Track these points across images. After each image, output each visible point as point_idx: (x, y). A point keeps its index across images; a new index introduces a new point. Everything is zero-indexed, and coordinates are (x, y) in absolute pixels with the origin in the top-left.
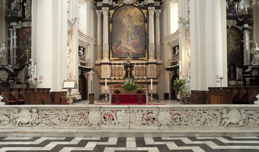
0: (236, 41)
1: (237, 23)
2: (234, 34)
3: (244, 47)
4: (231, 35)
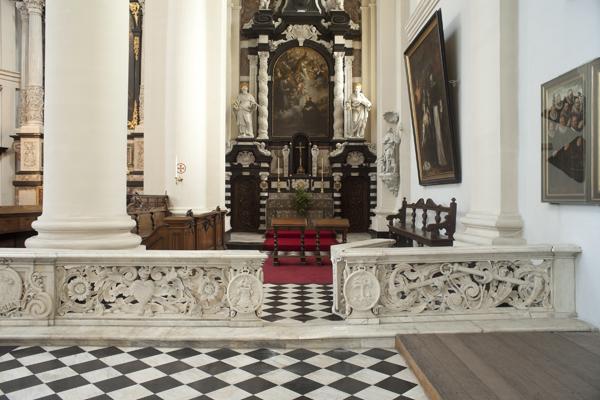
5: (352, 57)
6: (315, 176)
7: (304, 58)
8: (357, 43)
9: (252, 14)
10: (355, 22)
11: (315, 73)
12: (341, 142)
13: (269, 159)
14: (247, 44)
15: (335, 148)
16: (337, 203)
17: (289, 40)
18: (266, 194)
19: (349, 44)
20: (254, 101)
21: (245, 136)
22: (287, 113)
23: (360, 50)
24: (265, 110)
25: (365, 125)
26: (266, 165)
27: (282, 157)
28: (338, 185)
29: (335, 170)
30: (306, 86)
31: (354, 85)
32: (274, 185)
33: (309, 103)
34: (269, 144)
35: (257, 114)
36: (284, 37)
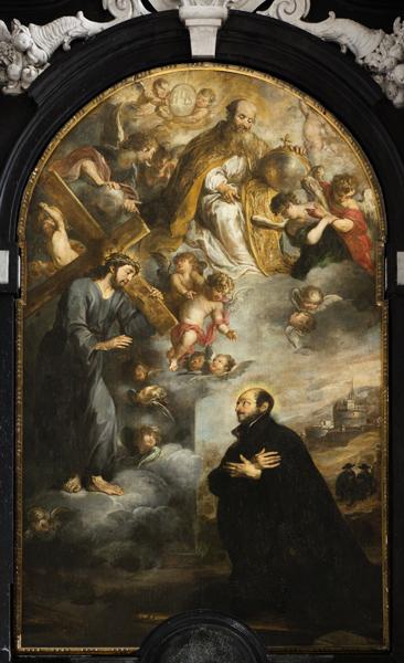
0: (319, 275)
2: (278, 157)
4: (235, 165)
7: (222, 136)
11: (296, 233)
17: (122, 15)
33: (257, 431)
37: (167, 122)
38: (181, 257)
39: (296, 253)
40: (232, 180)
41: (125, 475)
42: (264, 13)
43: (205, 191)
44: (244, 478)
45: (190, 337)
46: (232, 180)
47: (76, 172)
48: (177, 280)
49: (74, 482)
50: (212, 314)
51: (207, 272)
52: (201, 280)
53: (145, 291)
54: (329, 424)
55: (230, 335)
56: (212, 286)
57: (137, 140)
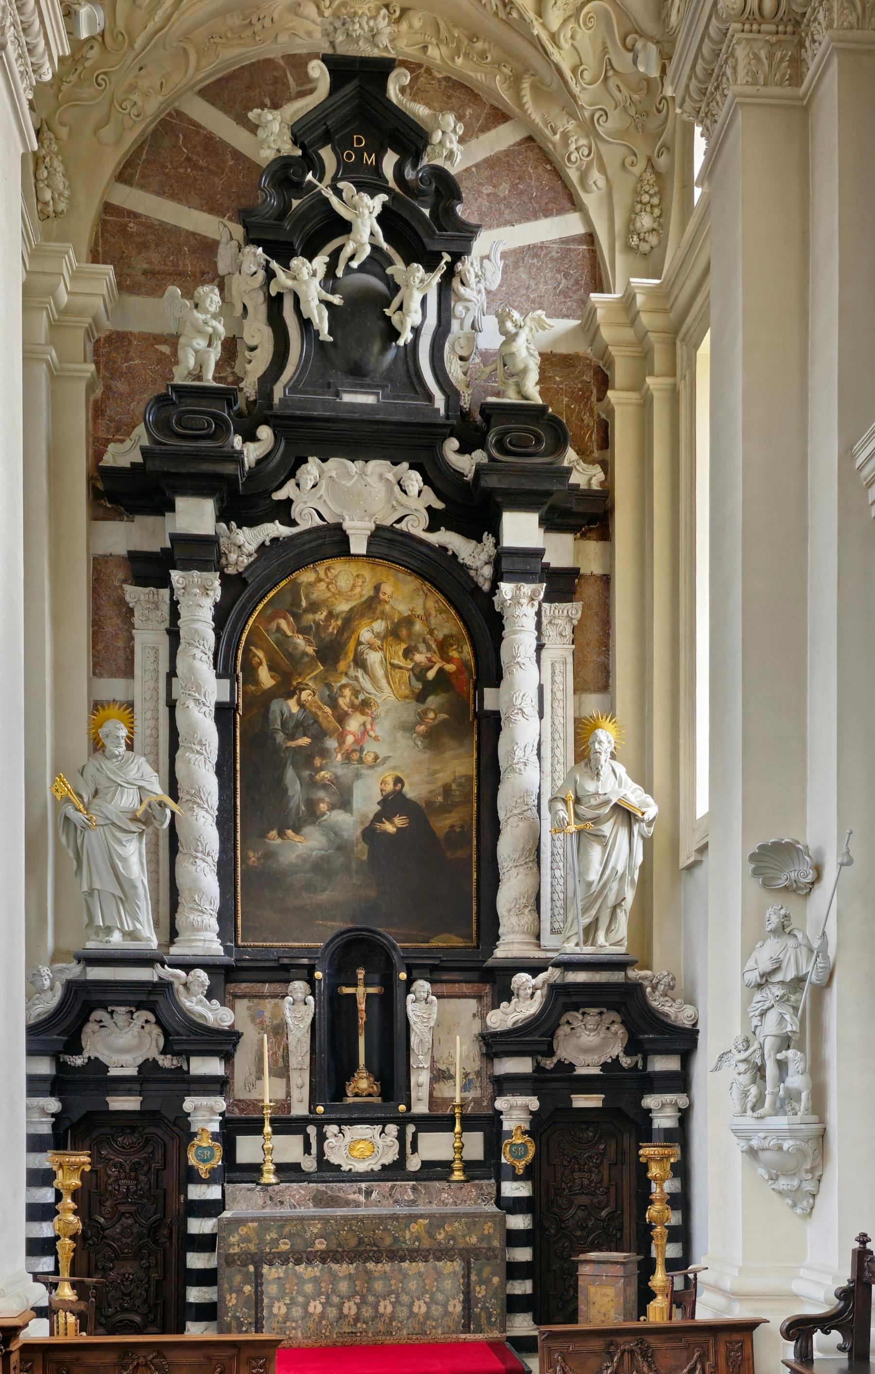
0: (432, 701)
1: (439, 505)
2: (408, 621)
3: (503, 764)
4: (379, 626)
5: (573, 610)
6: (420, 1108)
7: (371, 606)
8: (593, 547)
9: (140, 404)
10: (582, 453)
11: (419, 673)
12: (535, 970)
13: (224, 1043)
14: (125, 536)
15: (505, 994)
16: (519, 1222)
17: (304, 525)
18: (214, 1193)
19: (560, 550)
20: (157, 788)
21: (116, 938)
22: (302, 846)
23: (607, 580)
24: (204, 827)
25: (630, 895)
26: (213, 1067)
27: (279, 1030)
28: (519, 1149)
29: (504, 1085)
30: (381, 729)
31: (583, 732)
32: (247, 1149)
33: (393, 803)
34: (226, 977)
35: (174, 843)
36: (283, 511)
37: (334, 595)
38: (344, 686)
39: (419, 686)
40: (377, 636)
41: (308, 830)
42: (397, 526)
43: (359, 643)
44: (385, 833)
45: (350, 739)
46: (377, 636)
47: (274, 626)
48: (341, 701)
49: (274, 833)
50: (364, 724)
51: (361, 697)
52: (357, 702)
53: (320, 708)
54: (440, 799)
55: (376, 739)
56: (364, 706)
57: (314, 607)
